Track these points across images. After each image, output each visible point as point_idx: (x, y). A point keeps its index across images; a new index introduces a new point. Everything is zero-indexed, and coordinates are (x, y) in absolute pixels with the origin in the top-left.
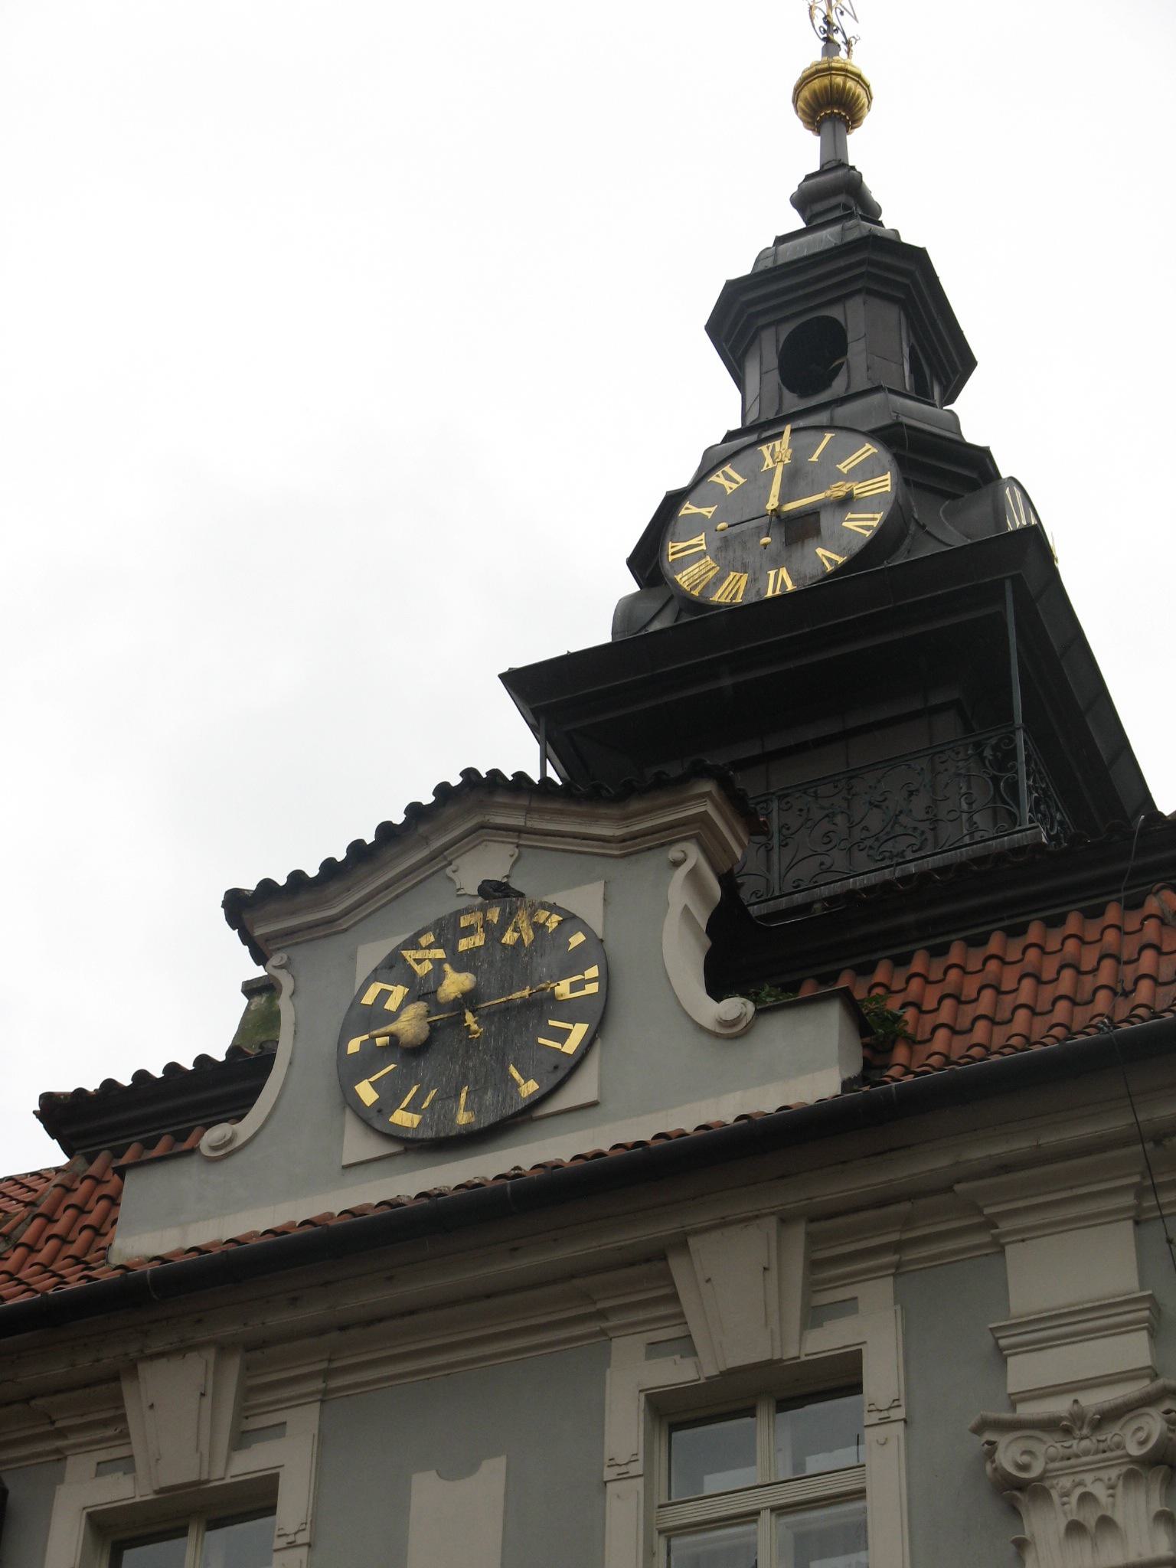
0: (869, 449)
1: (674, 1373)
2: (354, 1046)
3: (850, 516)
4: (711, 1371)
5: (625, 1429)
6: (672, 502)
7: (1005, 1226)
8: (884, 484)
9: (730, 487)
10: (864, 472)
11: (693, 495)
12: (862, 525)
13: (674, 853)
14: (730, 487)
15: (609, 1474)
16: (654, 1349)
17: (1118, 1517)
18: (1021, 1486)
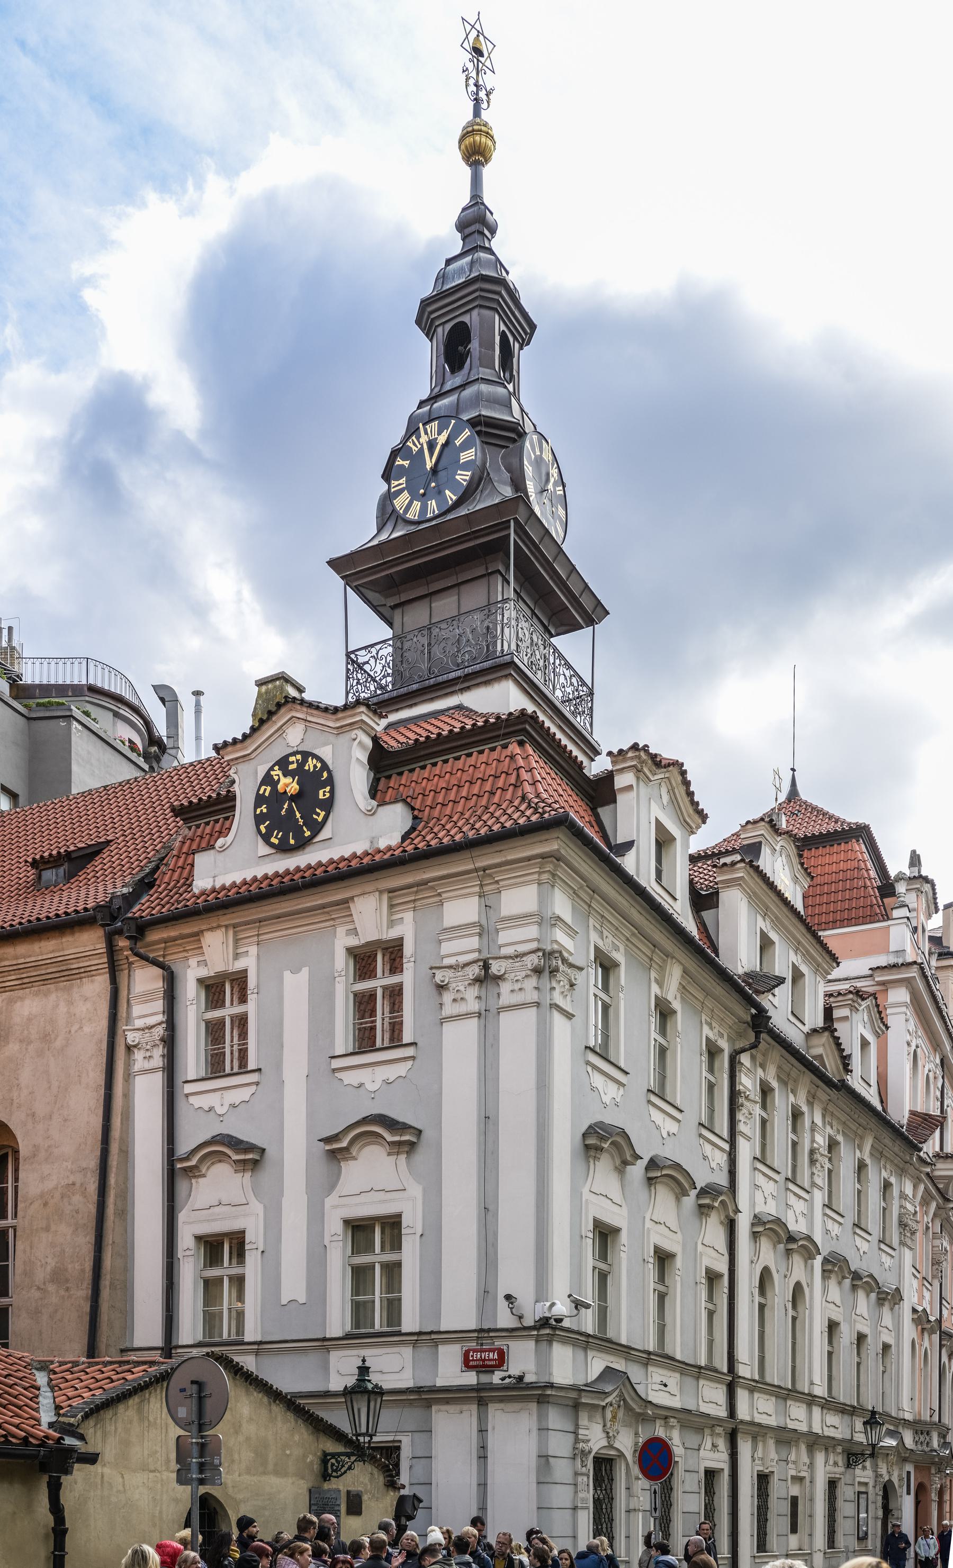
0: (467, 433)
3: (459, 472)
10: (466, 446)
17: (466, 997)
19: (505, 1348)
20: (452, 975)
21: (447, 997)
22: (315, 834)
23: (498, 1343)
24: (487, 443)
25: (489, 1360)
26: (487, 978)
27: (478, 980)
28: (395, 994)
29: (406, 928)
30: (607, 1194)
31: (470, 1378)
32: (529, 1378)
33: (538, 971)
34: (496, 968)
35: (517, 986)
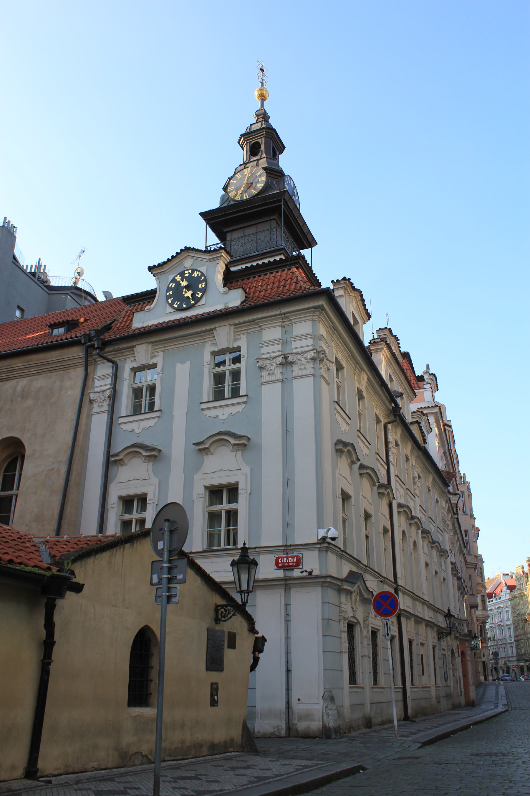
1: (215, 349)
2: (168, 294)
4: (220, 348)
5: (207, 357)
6: (230, 179)
7: (263, 327)
8: (264, 178)
9: (239, 177)
10: (260, 176)
11: (233, 179)
12: (260, 186)
13: (217, 262)
14: (239, 177)
15: (205, 364)
18: (262, 368)
19: (301, 555)
20: (267, 362)
21: (264, 373)
24: (269, 177)
25: (291, 562)
27: (281, 364)
29: (243, 342)
30: (344, 476)
31: (280, 574)
32: (316, 573)
33: (313, 359)
34: (290, 358)
35: (302, 367)
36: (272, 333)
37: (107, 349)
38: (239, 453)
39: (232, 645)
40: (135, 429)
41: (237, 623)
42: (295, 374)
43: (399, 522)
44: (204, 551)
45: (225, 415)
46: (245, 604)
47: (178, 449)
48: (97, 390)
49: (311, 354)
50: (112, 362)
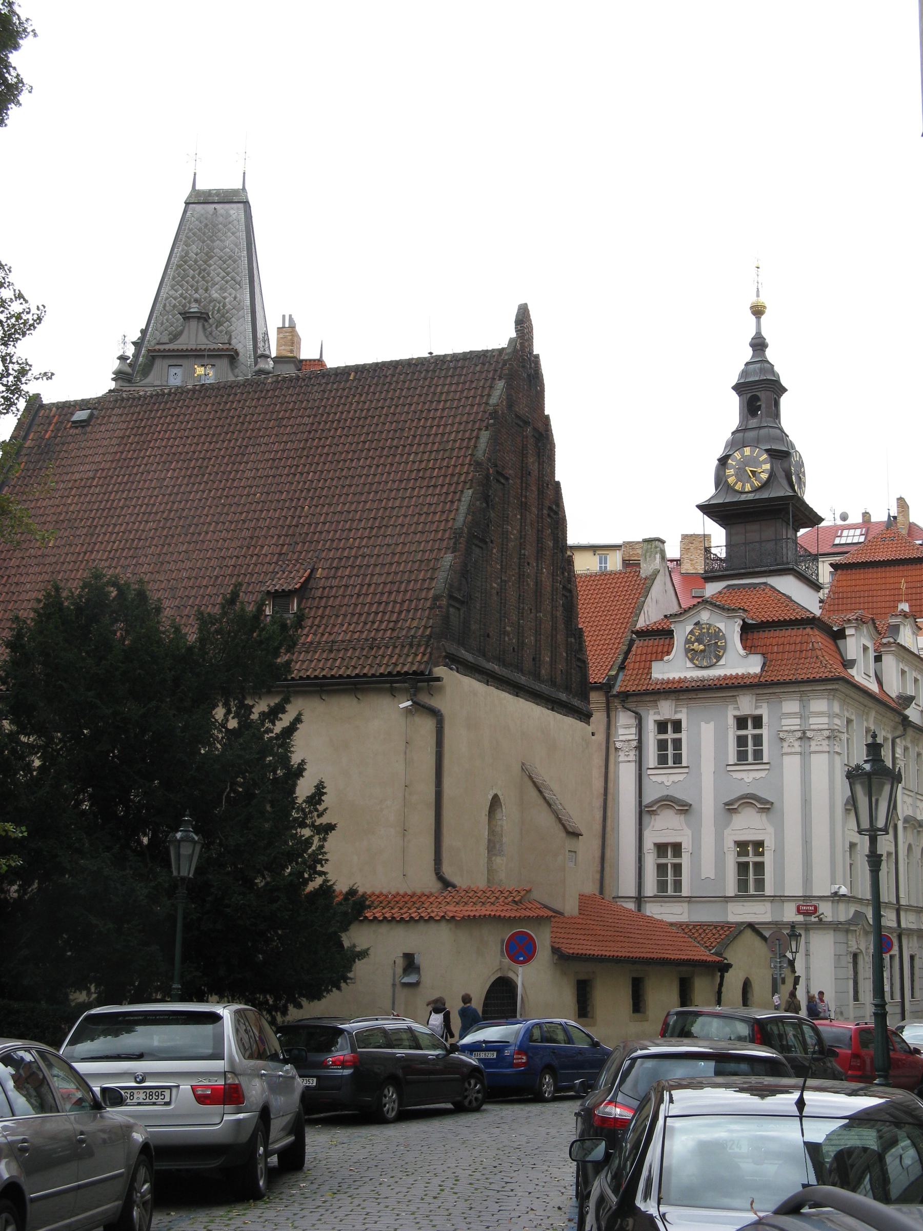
0: (765, 456)
10: (764, 462)
12: (764, 476)
16: (735, 709)
21: (785, 744)
22: (718, 661)
23: (814, 903)
26: (804, 738)
28: (758, 740)
29: (764, 711)
31: (800, 918)
33: (828, 737)
34: (809, 734)
36: (791, 706)
37: (630, 699)
38: (764, 814)
39: (783, 982)
40: (663, 782)
41: (787, 972)
42: (813, 748)
43: (905, 837)
44: (736, 896)
45: (749, 778)
46: (794, 959)
47: (708, 807)
48: (621, 738)
49: (826, 733)
50: (636, 713)
